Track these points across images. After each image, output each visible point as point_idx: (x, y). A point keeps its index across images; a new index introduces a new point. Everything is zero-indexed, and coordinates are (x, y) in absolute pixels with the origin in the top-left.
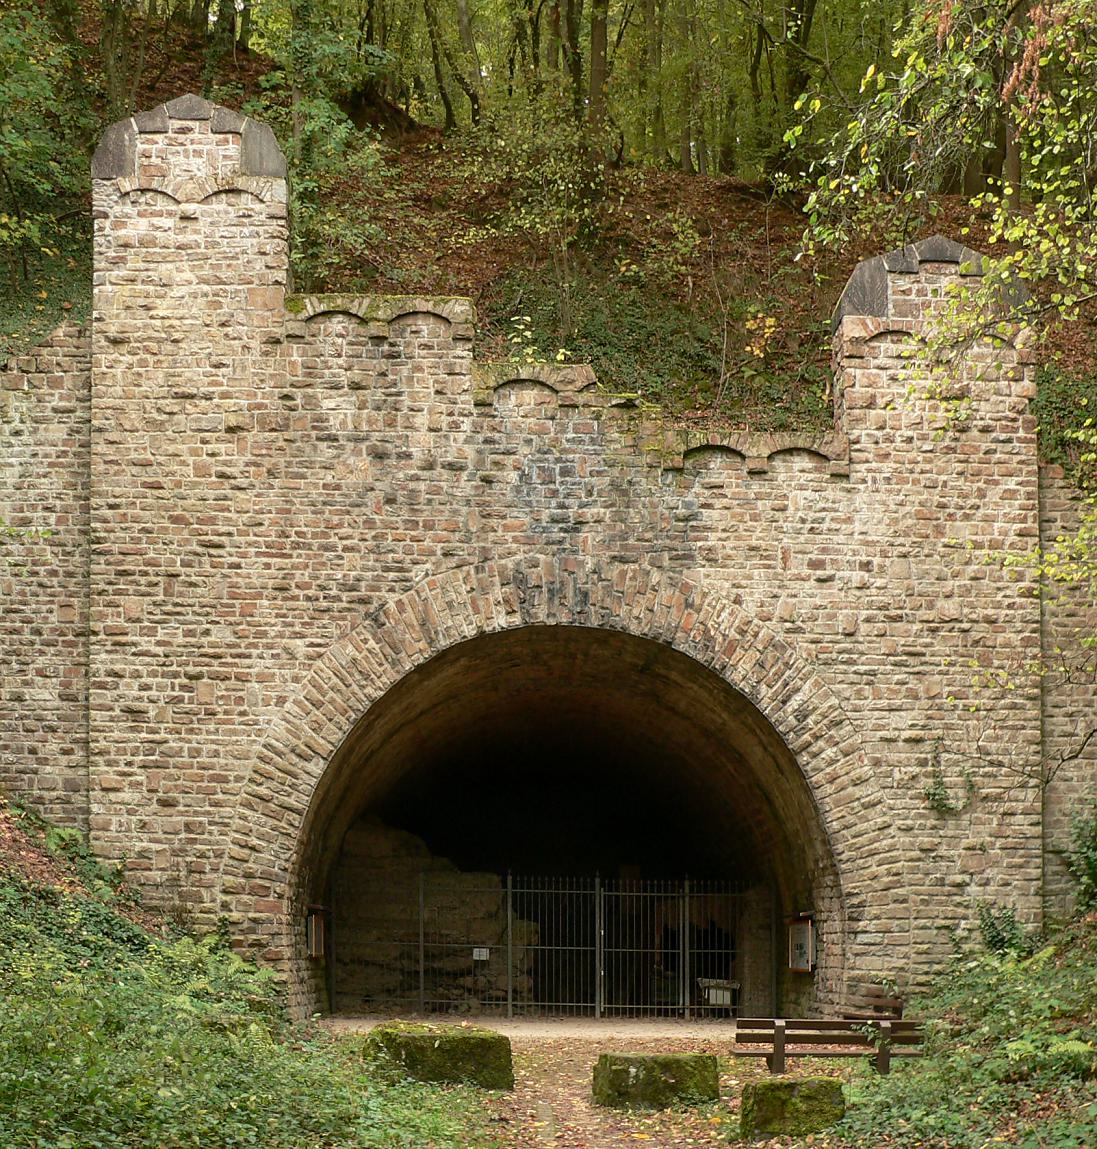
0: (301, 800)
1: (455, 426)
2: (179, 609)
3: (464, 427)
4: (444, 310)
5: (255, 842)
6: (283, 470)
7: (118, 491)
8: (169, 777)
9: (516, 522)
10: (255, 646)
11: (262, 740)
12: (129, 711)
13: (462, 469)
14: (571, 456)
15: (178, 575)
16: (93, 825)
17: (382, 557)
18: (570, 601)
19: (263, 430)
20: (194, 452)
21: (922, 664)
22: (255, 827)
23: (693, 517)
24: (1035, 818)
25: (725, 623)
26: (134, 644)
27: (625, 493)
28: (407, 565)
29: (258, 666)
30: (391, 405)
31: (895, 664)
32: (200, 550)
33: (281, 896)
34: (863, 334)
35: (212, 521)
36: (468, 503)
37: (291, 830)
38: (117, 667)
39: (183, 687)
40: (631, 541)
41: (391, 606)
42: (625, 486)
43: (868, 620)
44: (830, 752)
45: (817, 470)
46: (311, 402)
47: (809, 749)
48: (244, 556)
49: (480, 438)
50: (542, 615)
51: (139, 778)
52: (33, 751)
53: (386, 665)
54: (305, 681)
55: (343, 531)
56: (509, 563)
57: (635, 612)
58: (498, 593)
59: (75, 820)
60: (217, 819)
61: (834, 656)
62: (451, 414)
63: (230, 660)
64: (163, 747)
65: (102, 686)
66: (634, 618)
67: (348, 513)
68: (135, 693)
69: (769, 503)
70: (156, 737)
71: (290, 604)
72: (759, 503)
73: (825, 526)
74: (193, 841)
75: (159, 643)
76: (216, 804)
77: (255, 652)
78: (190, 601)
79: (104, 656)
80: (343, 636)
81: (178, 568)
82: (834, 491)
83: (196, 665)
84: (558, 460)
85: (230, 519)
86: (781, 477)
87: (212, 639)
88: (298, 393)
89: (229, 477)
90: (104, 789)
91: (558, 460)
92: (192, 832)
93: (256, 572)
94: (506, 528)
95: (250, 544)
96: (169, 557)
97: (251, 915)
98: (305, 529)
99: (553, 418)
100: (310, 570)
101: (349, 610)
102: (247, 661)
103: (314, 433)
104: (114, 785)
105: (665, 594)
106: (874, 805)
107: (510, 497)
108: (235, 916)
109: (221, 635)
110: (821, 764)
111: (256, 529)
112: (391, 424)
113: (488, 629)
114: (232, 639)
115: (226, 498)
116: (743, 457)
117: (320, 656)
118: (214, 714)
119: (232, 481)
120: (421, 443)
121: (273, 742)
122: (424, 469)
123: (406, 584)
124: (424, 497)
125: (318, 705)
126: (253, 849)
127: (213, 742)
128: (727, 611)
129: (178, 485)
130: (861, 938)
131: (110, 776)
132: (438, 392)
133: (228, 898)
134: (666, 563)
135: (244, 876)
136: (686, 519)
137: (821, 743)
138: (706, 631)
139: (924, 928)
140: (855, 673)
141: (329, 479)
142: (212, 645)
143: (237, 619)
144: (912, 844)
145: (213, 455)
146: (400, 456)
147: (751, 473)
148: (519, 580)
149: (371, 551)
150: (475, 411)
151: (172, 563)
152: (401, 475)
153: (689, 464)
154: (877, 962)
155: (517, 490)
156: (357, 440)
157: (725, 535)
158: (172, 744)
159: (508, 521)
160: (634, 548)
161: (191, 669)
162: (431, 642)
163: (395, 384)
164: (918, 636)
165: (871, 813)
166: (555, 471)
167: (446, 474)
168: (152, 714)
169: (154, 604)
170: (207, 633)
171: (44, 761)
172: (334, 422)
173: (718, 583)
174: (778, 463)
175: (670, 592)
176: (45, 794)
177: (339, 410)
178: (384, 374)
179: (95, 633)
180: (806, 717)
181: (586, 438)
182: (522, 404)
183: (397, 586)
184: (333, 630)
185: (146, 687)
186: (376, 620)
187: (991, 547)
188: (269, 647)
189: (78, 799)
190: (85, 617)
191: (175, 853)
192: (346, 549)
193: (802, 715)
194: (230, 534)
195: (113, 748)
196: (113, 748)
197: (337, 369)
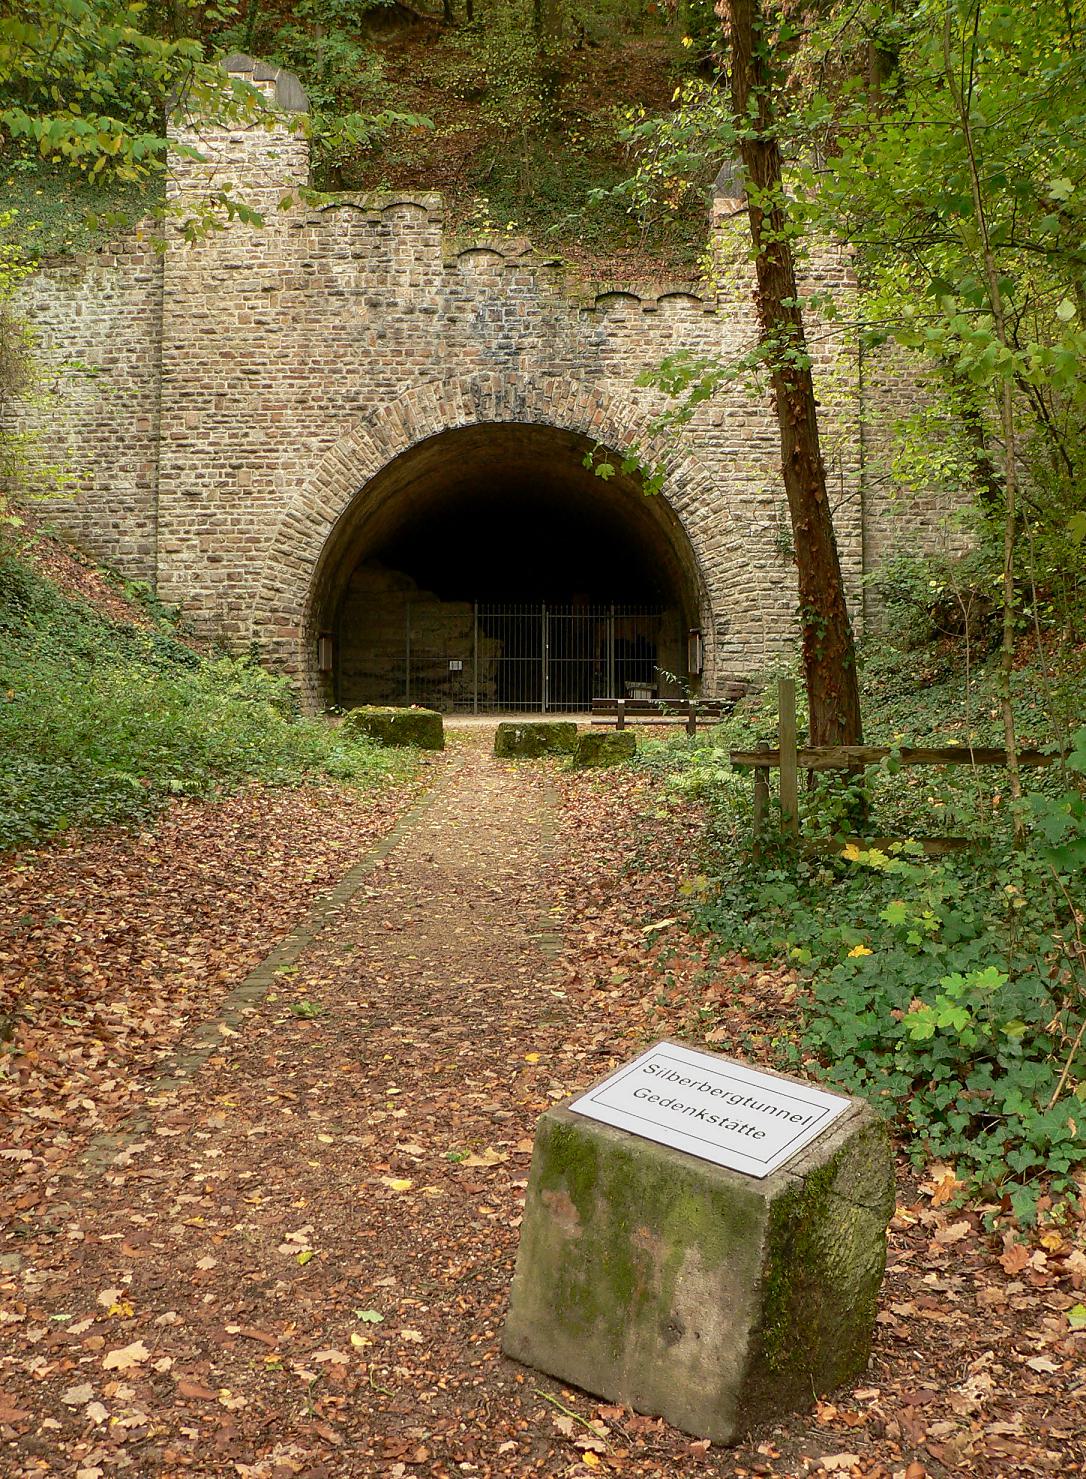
0: (313, 554)
1: (429, 283)
2: (226, 419)
3: (435, 283)
4: (422, 201)
5: (279, 585)
6: (303, 317)
7: (182, 336)
8: (217, 541)
9: (474, 349)
10: (281, 443)
11: (285, 511)
12: (188, 494)
13: (434, 312)
14: (513, 302)
15: (224, 395)
16: (159, 577)
17: (375, 377)
18: (512, 404)
19: (289, 289)
20: (239, 307)
21: (772, 446)
22: (279, 575)
23: (603, 343)
24: (857, 559)
25: (626, 418)
26: (192, 445)
27: (553, 327)
28: (393, 382)
29: (283, 457)
30: (383, 269)
31: (752, 447)
32: (242, 376)
33: (297, 625)
34: (728, 211)
35: (251, 355)
36: (438, 336)
37: (306, 576)
38: (180, 462)
39: (228, 475)
40: (557, 361)
41: (382, 411)
42: (553, 322)
43: (731, 415)
44: (703, 511)
45: (693, 308)
46: (324, 268)
47: (688, 509)
48: (274, 379)
49: (448, 290)
50: (491, 415)
51: (194, 542)
52: (116, 526)
53: (378, 454)
54: (318, 467)
55: (347, 359)
56: (468, 378)
57: (560, 411)
58: (459, 400)
59: (145, 575)
60: (251, 570)
61: (706, 441)
62: (426, 274)
63: (263, 454)
64: (213, 519)
65: (168, 476)
66: (559, 416)
67: (351, 346)
68: (193, 481)
69: (658, 332)
70: (208, 511)
71: (307, 412)
72: (651, 332)
73: (699, 348)
74: (234, 587)
75: (210, 444)
76: (251, 559)
77: (281, 447)
78: (234, 413)
79: (170, 455)
80: (346, 434)
81: (226, 389)
82: (706, 323)
83: (237, 458)
84: (503, 305)
85: (265, 353)
86: (667, 314)
87: (250, 439)
88: (316, 263)
89: (264, 324)
90: (168, 552)
91: (503, 305)
92: (233, 580)
93: (282, 390)
94: (466, 354)
95: (278, 371)
96: (219, 381)
97: (275, 639)
98: (319, 359)
99: (500, 275)
100: (322, 387)
101: (351, 415)
102: (276, 454)
103: (326, 290)
104: (176, 548)
105: (581, 398)
106: (737, 549)
107: (469, 331)
108: (263, 640)
109: (257, 436)
110: (697, 519)
111: (283, 360)
112: (383, 282)
113: (451, 426)
114: (264, 439)
115: (261, 338)
116: (639, 300)
117: (329, 448)
118: (250, 494)
119: (266, 327)
120: (404, 295)
121: (294, 512)
122: (406, 313)
123: (392, 396)
124: (406, 333)
125: (326, 484)
126: (277, 590)
127: (250, 513)
128: (628, 409)
129: (227, 330)
130: (727, 647)
131: (172, 541)
132: (416, 259)
133: (258, 628)
134: (583, 376)
135: (270, 611)
136: (598, 345)
137: (696, 504)
138: (612, 424)
139: (774, 640)
140: (722, 453)
141: (337, 322)
142: (250, 444)
143: (269, 424)
144: (765, 577)
145: (252, 308)
146: (388, 305)
147: (645, 311)
148: (475, 390)
149: (367, 373)
150: (444, 272)
151: (222, 386)
152: (389, 318)
153: (599, 305)
154: (738, 665)
155: (474, 326)
156: (358, 294)
157: (626, 355)
158: (219, 516)
159: (468, 349)
160: (559, 366)
161: (234, 461)
162: (410, 436)
163: (386, 254)
164: (767, 426)
165: (733, 555)
166: (501, 313)
167: (422, 316)
168: (205, 495)
169: (208, 415)
170: (246, 435)
171: (123, 533)
172: (341, 282)
173: (620, 390)
174: (665, 304)
175: (585, 396)
176: (124, 556)
177: (345, 273)
178: (378, 247)
179: (164, 439)
180: (685, 485)
181: (525, 288)
182: (476, 268)
183: (386, 397)
184: (339, 430)
185: (201, 476)
186: (370, 422)
187: (823, 362)
188: (292, 443)
189: (148, 559)
190: (157, 427)
191: (220, 596)
192: (348, 372)
193: (682, 484)
194: (264, 364)
195: (175, 521)
196: (175, 521)
197: (343, 245)
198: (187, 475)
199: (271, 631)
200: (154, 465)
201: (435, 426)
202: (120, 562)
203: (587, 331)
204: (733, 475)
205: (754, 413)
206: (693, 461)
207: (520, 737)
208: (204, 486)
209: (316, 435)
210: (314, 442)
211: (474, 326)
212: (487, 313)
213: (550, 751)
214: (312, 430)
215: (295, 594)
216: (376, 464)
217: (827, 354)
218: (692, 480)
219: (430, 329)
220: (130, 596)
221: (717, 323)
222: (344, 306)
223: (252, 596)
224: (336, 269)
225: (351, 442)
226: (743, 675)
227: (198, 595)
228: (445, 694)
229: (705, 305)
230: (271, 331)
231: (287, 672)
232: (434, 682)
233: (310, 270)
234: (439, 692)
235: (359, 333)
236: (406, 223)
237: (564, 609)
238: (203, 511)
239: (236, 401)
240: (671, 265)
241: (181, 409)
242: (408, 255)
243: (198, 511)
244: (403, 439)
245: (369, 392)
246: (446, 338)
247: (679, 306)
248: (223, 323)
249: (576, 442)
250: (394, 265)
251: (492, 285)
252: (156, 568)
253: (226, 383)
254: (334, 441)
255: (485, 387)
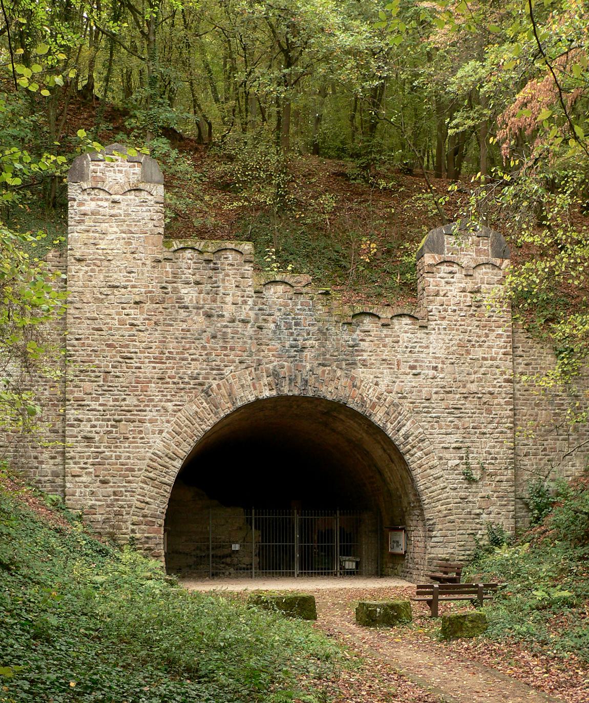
0: (171, 480)
1: (245, 302)
2: (110, 388)
3: (249, 303)
4: (240, 248)
5: (148, 500)
6: (162, 322)
7: (80, 332)
8: (106, 469)
9: (274, 347)
10: (148, 406)
11: (151, 451)
12: (86, 438)
13: (248, 322)
14: (299, 317)
15: (110, 372)
16: (67, 493)
17: (210, 364)
18: (299, 384)
19: (152, 303)
20: (118, 314)
21: (461, 413)
22: (148, 493)
23: (357, 345)
24: (511, 483)
25: (371, 394)
26: (88, 405)
27: (325, 334)
28: (221, 368)
29: (150, 416)
30: (214, 293)
31: (448, 413)
32: (121, 360)
33: (160, 526)
34: (434, 262)
35: (127, 346)
36: (251, 338)
37: (166, 494)
38: (80, 417)
39: (112, 426)
40: (328, 356)
41: (214, 386)
42: (325, 331)
43: (436, 393)
44: (419, 454)
45: (413, 324)
46: (175, 290)
47: (410, 452)
48: (143, 363)
49: (257, 308)
50: (286, 391)
51: (91, 470)
52: (36, 458)
53: (212, 415)
54: (172, 422)
55: (191, 351)
56: (271, 366)
57: (330, 389)
58: (265, 380)
59: (57, 491)
60: (129, 489)
61: (421, 409)
62: (243, 297)
63: (136, 413)
64: (102, 455)
65: (72, 426)
66: (329, 392)
67: (194, 343)
68: (89, 429)
69: (391, 339)
70: (99, 450)
71: (165, 386)
72: (387, 339)
73: (416, 350)
74: (118, 500)
75: (100, 405)
76: (129, 482)
77: (148, 409)
78: (116, 385)
79: (73, 411)
80: (191, 401)
81: (110, 369)
82: (420, 334)
83: (119, 415)
84: (293, 319)
85: (136, 346)
86: (397, 327)
87: (127, 402)
88: (169, 286)
89: (136, 325)
90: (73, 476)
91: (293, 319)
92: (117, 496)
93: (148, 370)
94: (269, 350)
95: (146, 357)
96: (106, 364)
97: (146, 535)
98: (172, 350)
99: (291, 299)
100: (175, 370)
101: (194, 388)
102: (144, 413)
103: (177, 305)
104: (78, 474)
105: (343, 381)
106: (439, 478)
107: (271, 336)
108: (138, 535)
109: (131, 401)
110: (415, 459)
111: (149, 350)
112: (214, 301)
113: (260, 397)
114: (136, 403)
115: (134, 335)
116: (379, 318)
117: (180, 410)
118: (128, 439)
119: (137, 327)
120: (229, 310)
121: (157, 452)
122: (230, 322)
123: (221, 376)
124: (230, 336)
125: (178, 434)
126: (147, 503)
127: (127, 452)
128: (372, 389)
129: (110, 329)
130: (434, 539)
131: (76, 469)
132: (237, 286)
133: (134, 527)
134: (344, 367)
135: (143, 516)
136: (353, 346)
137: (415, 449)
138: (362, 398)
139: (462, 534)
140: (431, 417)
141: (184, 326)
142: (127, 406)
143: (139, 393)
144: (457, 496)
145: (128, 315)
146: (219, 316)
147: (383, 325)
148: (275, 374)
149: (204, 361)
150: (254, 295)
151: (107, 366)
152: (219, 325)
153: (354, 321)
154: (440, 550)
155: (274, 332)
156: (198, 308)
157: (371, 354)
158: (107, 453)
159: (270, 347)
160: (329, 360)
161: (116, 417)
162: (233, 404)
163: (216, 282)
164: (458, 400)
165: (438, 481)
166: (292, 324)
167: (240, 325)
168: (97, 439)
169: (98, 386)
170: (124, 400)
171: (42, 463)
172: (187, 300)
173: (368, 376)
174: (395, 321)
175: (345, 380)
176: (43, 479)
177: (189, 294)
178: (211, 278)
179: (69, 400)
180: (408, 438)
181: (307, 308)
182: (275, 293)
183: (217, 377)
184: (186, 398)
185: (94, 426)
186: (207, 393)
187: (491, 360)
188: (155, 406)
189: (59, 481)
190: (64, 393)
191: (108, 506)
192: (193, 360)
193: (406, 437)
194: (136, 353)
195: (77, 455)
196: (77, 455)
197: (188, 275)
198: (85, 425)
199: (143, 530)
200: (61, 418)
201: (249, 397)
202: (39, 482)
203: (346, 337)
204: (437, 431)
205: (450, 392)
206: (413, 422)
207: (380, 612)
208: (97, 433)
209: (171, 401)
210: (170, 406)
211: (274, 332)
212: (283, 324)
213: (400, 622)
214: (169, 398)
215: (159, 506)
216: (211, 421)
217: (493, 355)
218: (412, 434)
219: (246, 333)
220: (48, 504)
221: (427, 334)
222: (189, 316)
223: (130, 506)
224: (183, 291)
225: (195, 406)
226: (444, 556)
227: (94, 505)
228: (227, 564)
229: (420, 322)
230: (140, 331)
231: (154, 556)
232: (220, 557)
233: (166, 290)
234: (223, 563)
235: (199, 334)
236: (229, 262)
237: (308, 513)
238: (96, 450)
239: (117, 377)
240: (368, 297)
241: (81, 381)
242: (231, 283)
243: (92, 449)
244: (229, 405)
245: (207, 374)
246: (256, 339)
247: (404, 322)
248: (108, 324)
249: (338, 409)
250: (221, 290)
251: (286, 305)
252: (64, 487)
253: (110, 364)
254: (183, 405)
255: (282, 372)
